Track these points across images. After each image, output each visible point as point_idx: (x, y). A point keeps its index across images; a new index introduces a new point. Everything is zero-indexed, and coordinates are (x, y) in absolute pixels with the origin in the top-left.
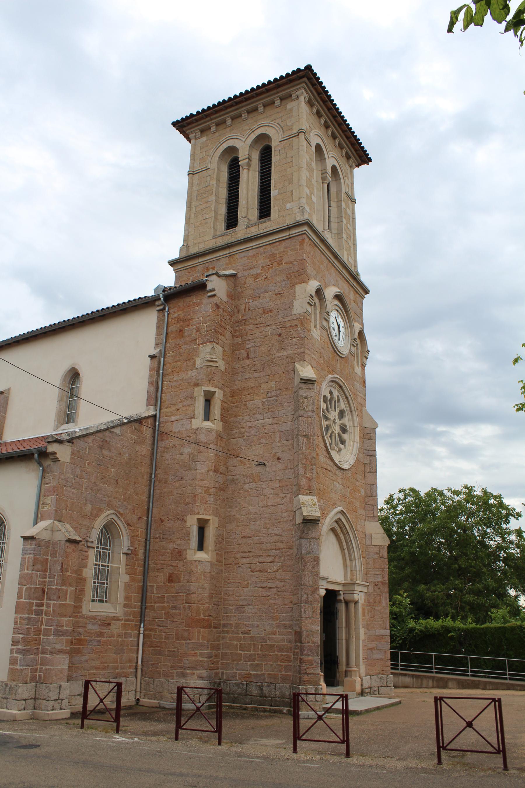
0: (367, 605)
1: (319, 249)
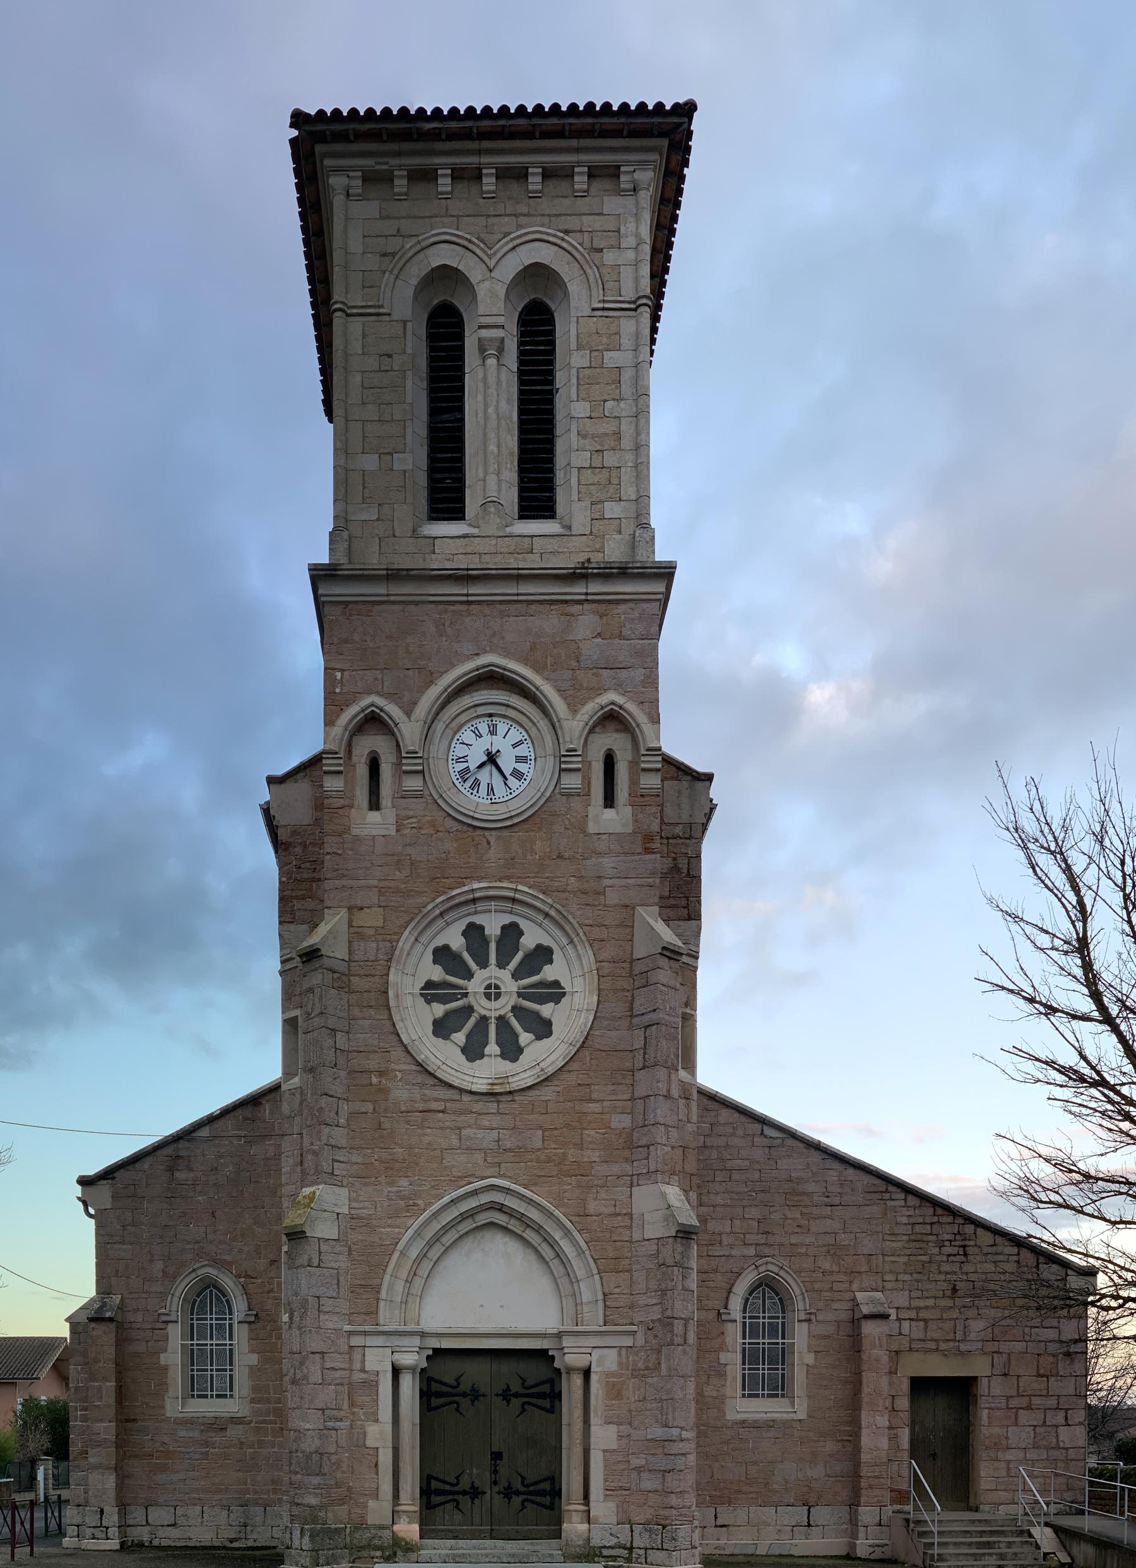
0: (632, 1374)
1: (393, 602)
